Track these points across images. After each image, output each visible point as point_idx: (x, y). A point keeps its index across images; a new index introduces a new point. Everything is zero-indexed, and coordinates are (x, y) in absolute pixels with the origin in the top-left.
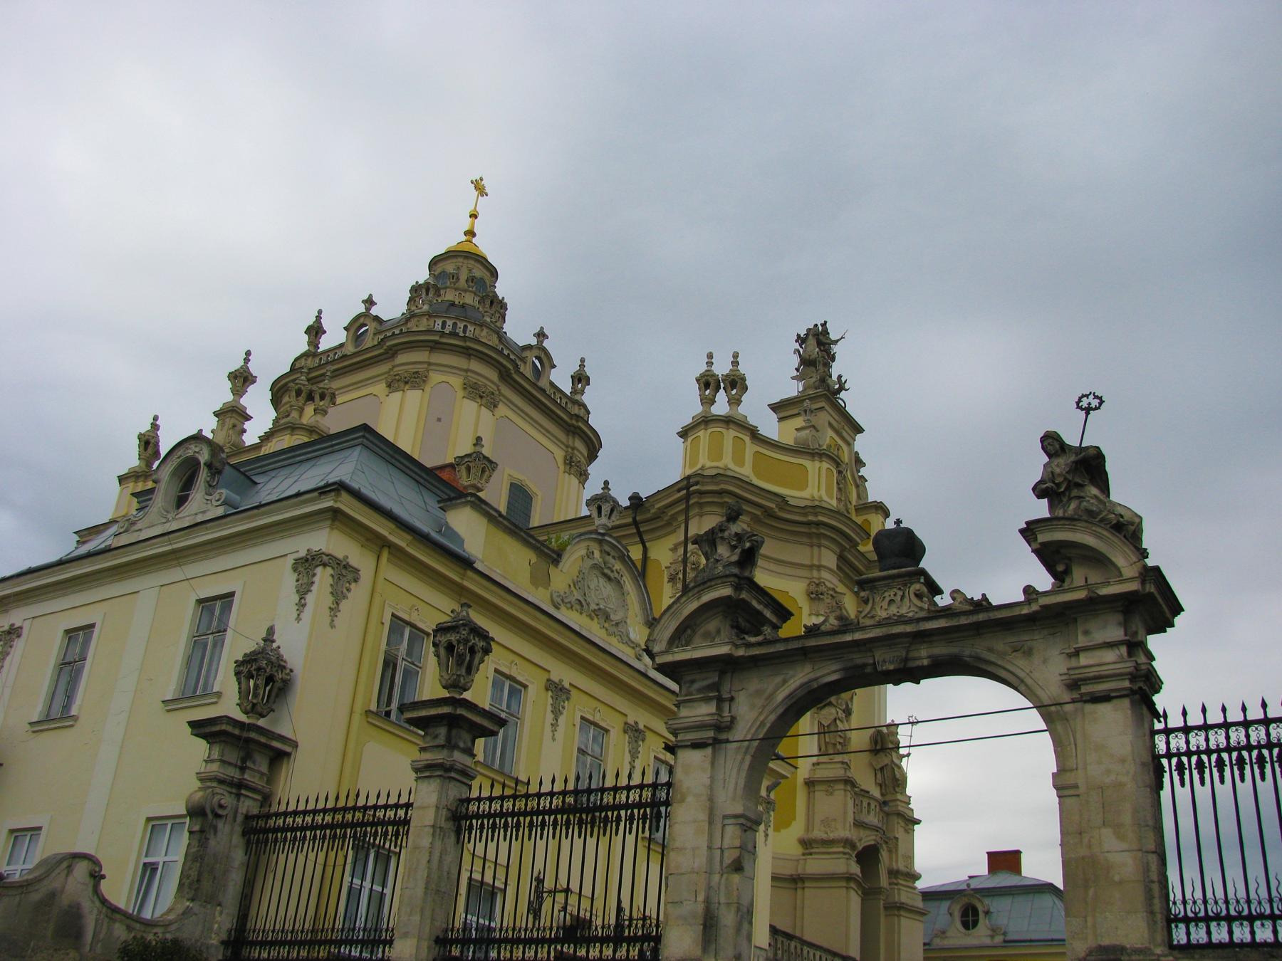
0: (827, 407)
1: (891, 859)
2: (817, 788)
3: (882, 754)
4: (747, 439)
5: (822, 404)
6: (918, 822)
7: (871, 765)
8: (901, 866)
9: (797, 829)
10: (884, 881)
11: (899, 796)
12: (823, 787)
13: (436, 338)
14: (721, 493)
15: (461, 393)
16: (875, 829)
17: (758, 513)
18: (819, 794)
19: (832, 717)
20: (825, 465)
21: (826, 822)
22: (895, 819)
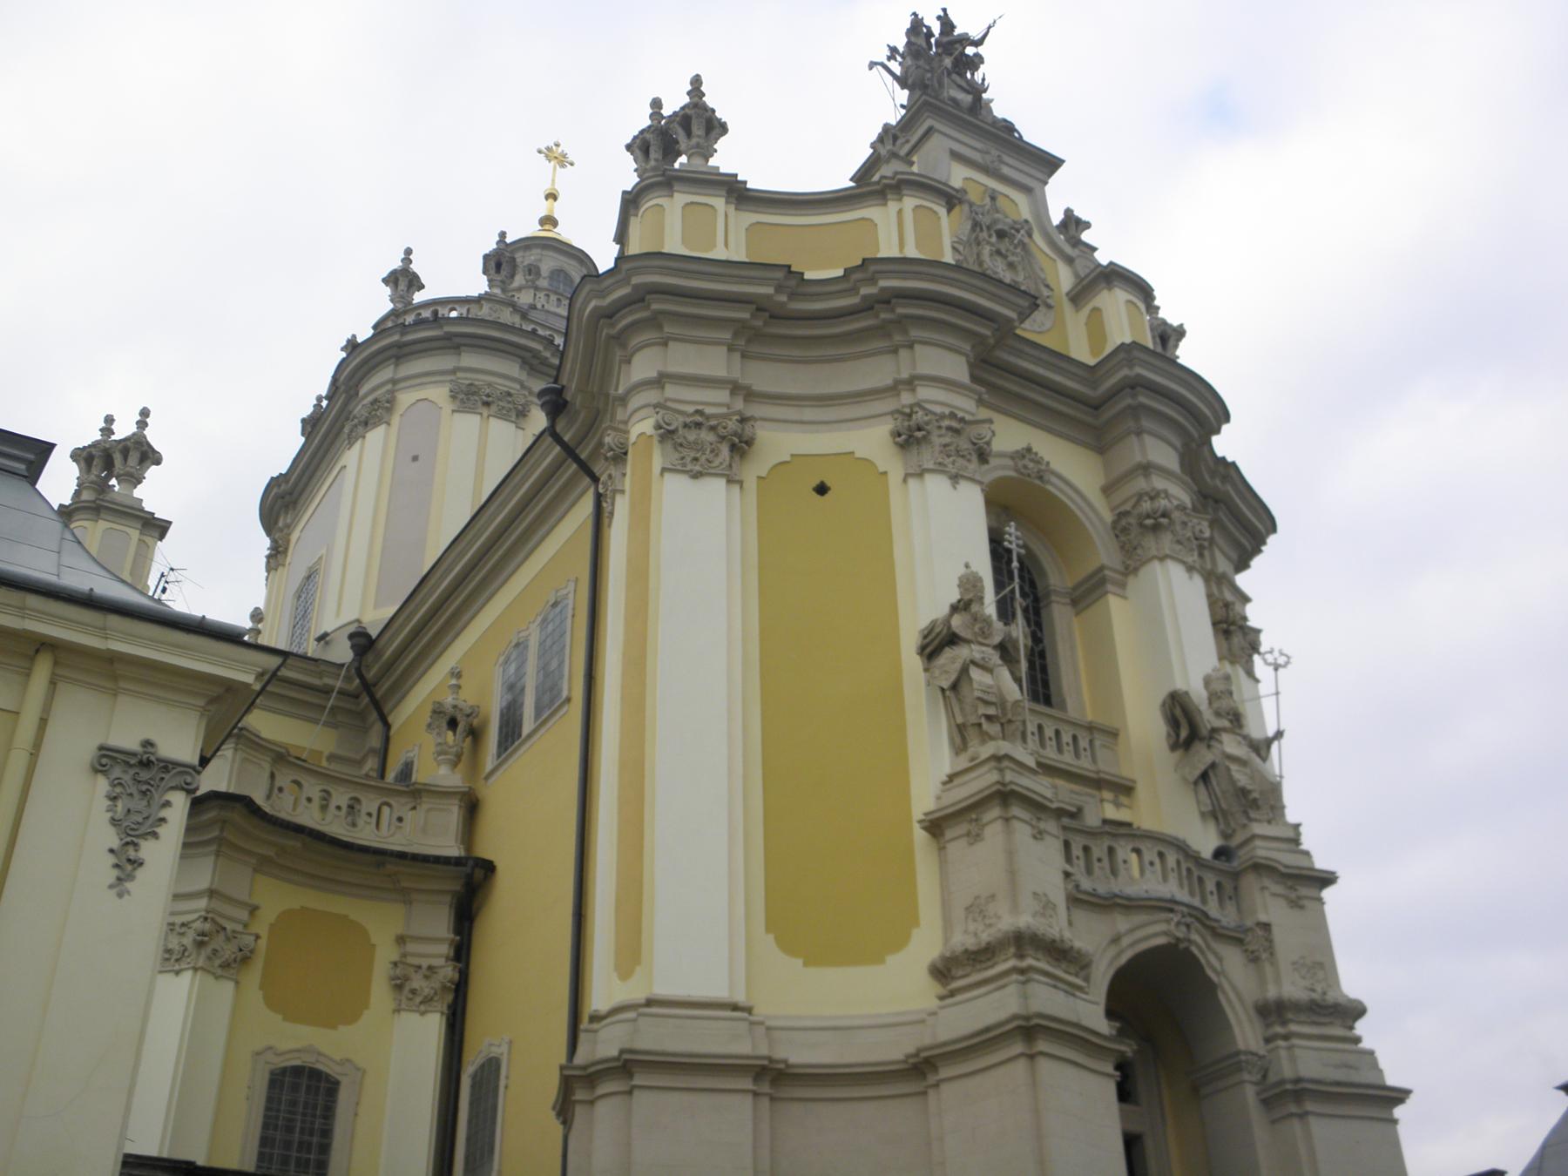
0: (938, 126)
1: (1262, 982)
2: (949, 834)
3: (1199, 748)
4: (719, 203)
5: (929, 123)
6: (1327, 879)
7: (1185, 779)
8: (1292, 988)
9: (927, 943)
10: (1246, 1034)
11: (1258, 829)
12: (962, 828)
13: (396, 338)
14: (640, 297)
15: (447, 406)
16: (1166, 906)
17: (744, 315)
18: (956, 849)
19: (958, 666)
20: (910, 202)
21: (976, 909)
22: (1250, 882)
